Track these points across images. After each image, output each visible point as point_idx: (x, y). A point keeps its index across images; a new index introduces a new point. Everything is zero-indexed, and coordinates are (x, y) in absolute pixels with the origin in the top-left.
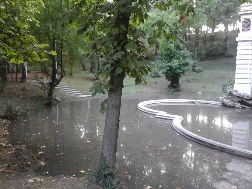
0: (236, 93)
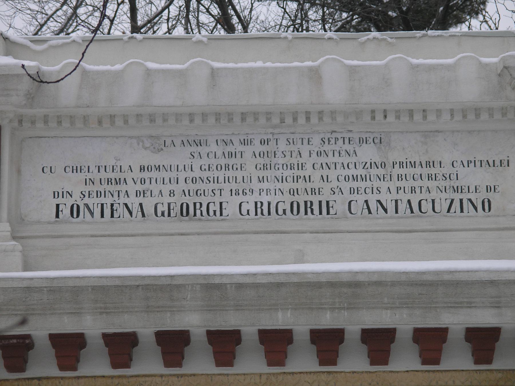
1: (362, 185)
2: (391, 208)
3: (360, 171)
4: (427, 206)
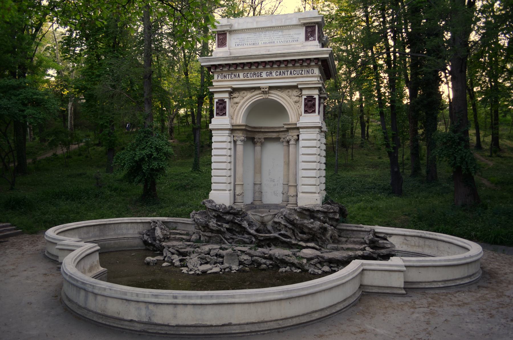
0: (210, 204)
4: (288, 41)
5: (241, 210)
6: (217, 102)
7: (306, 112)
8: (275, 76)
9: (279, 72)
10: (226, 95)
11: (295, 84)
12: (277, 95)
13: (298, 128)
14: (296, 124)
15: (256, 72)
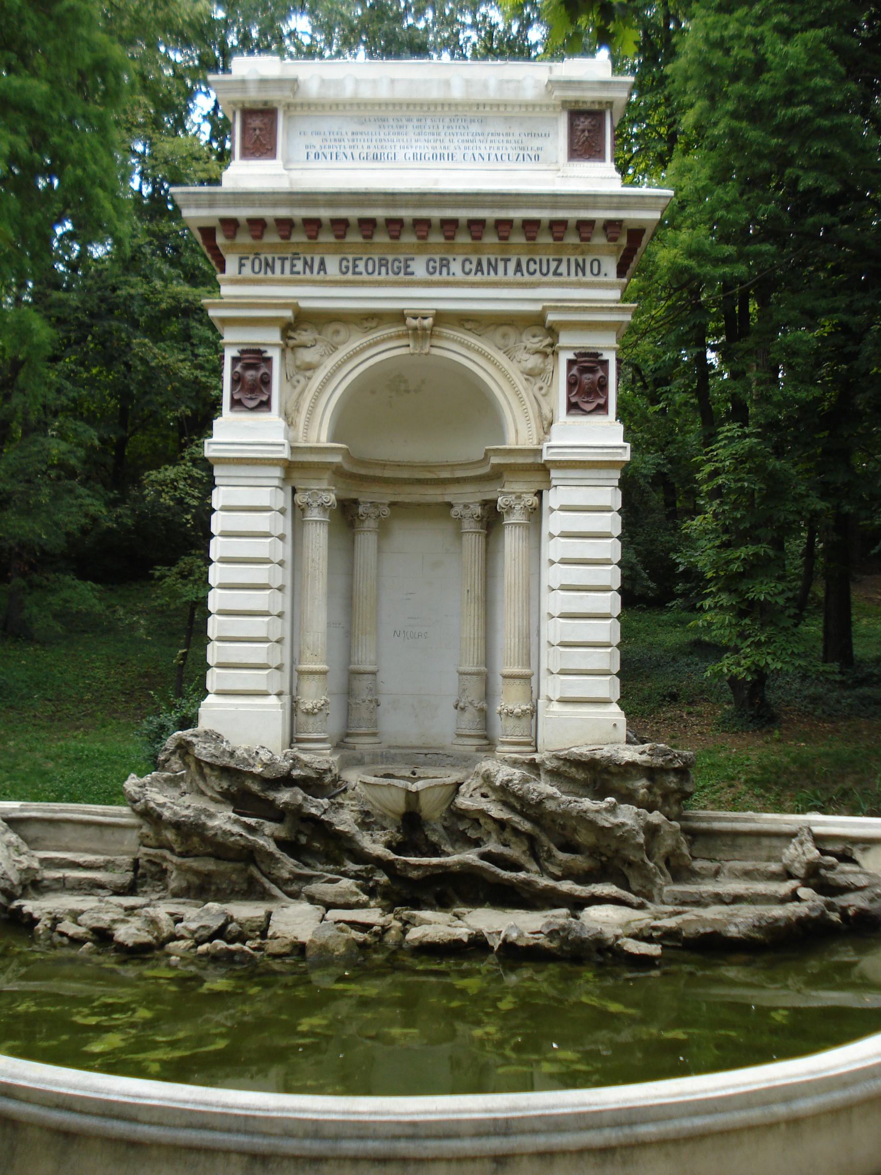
1: (471, 145)
2: (486, 158)
3: (470, 138)
4: (505, 157)
5: (330, 770)
6: (235, 360)
7: (573, 407)
8: (460, 276)
9: (475, 263)
10: (274, 336)
11: (537, 307)
12: (462, 344)
13: (544, 469)
14: (539, 452)
15: (390, 258)
